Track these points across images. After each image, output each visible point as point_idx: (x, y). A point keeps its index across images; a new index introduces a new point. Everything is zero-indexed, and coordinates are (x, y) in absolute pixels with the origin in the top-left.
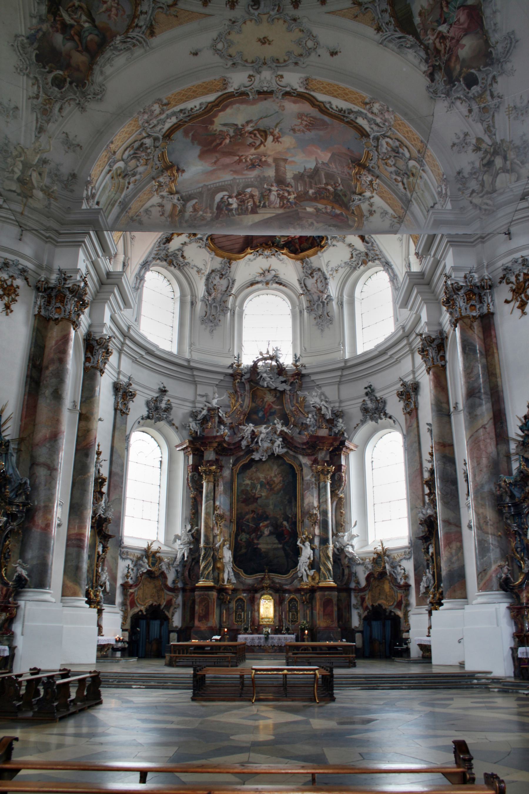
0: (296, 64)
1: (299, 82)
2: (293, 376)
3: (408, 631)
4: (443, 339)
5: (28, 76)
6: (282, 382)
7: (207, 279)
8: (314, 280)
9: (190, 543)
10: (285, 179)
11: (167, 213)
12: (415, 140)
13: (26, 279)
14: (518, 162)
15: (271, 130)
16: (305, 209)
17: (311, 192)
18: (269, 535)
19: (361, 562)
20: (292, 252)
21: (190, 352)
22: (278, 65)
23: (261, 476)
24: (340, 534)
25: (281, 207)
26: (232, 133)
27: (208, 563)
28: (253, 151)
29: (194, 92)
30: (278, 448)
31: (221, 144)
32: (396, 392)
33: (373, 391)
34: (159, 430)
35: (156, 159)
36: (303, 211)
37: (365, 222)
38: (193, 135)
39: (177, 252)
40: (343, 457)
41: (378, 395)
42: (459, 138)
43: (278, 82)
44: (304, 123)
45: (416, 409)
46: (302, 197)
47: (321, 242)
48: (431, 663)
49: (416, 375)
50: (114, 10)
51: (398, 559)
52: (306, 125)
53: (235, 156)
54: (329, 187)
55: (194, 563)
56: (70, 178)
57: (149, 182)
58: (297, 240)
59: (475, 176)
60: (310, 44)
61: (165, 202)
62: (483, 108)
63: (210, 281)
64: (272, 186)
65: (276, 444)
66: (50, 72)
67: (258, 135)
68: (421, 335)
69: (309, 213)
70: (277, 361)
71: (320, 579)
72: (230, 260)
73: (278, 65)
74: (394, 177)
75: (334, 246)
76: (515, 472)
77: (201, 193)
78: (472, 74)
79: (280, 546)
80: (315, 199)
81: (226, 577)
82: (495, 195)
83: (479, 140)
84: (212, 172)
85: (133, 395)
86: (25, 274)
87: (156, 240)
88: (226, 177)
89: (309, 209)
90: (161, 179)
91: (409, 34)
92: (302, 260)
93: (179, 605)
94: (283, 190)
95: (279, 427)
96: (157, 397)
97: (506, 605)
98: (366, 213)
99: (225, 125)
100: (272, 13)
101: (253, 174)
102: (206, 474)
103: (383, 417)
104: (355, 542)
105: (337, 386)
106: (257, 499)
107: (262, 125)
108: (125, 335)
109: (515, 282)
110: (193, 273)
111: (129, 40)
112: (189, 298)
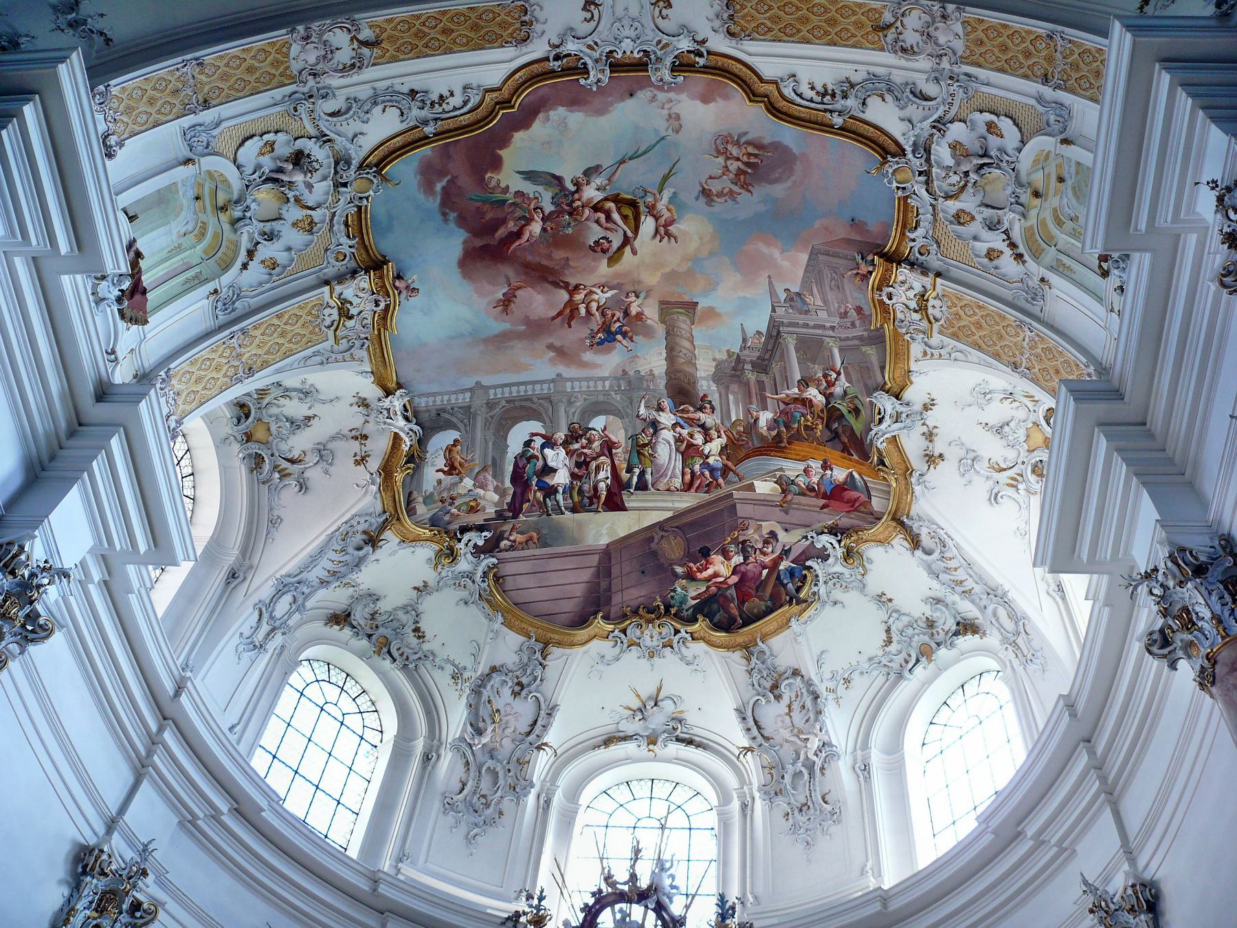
1: (711, 13)
7: (477, 691)
8: (782, 707)
10: (693, 382)
11: (374, 464)
15: (650, 199)
16: (751, 488)
17: (765, 417)
20: (718, 627)
25: (687, 487)
26: (549, 208)
28: (603, 269)
29: (445, 31)
31: (518, 234)
35: (339, 227)
36: (748, 494)
37: (917, 489)
38: (444, 188)
43: (660, 21)
44: (734, 166)
47: (798, 590)
52: (740, 172)
53: (556, 284)
54: (813, 393)
58: (733, 592)
61: (370, 429)
63: (486, 693)
64: (660, 409)
67: (616, 216)
69: (764, 502)
70: (660, 909)
75: (835, 603)
77: (467, 409)
80: (775, 446)
84: (500, 341)
87: (334, 528)
89: (764, 487)
90: (348, 290)
92: (747, 648)
94: (691, 422)
98: (917, 463)
99: (530, 176)
101: (609, 363)
108: (164, 717)
110: (440, 680)
112: (419, 745)
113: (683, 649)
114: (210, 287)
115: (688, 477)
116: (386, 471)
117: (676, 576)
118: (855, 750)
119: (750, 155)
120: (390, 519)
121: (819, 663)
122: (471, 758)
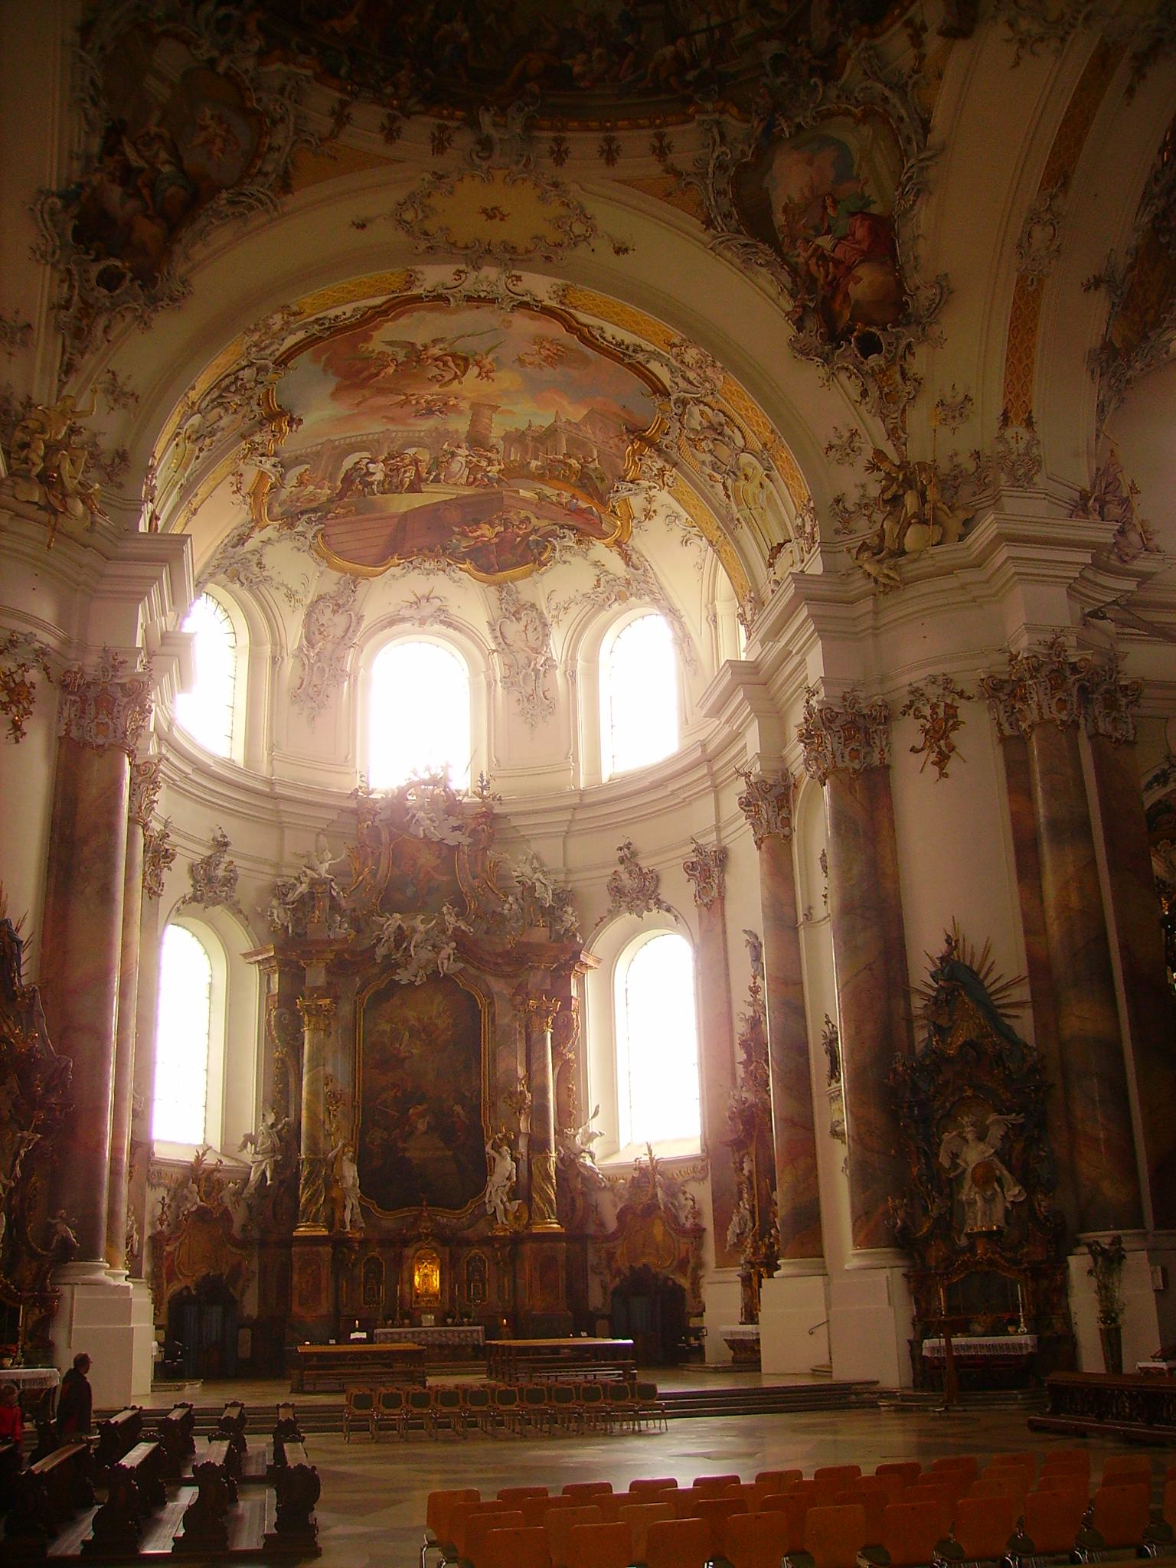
0: (548, 258)
2: (475, 817)
3: (701, 1315)
4: (787, 787)
5: (54, 266)
6: (454, 829)
7: (309, 615)
8: (521, 626)
9: (274, 1150)
12: (758, 425)
13: (46, 669)
14: (945, 507)
15: (478, 357)
16: (518, 492)
17: (534, 464)
18: (426, 1133)
19: (608, 1184)
21: (271, 762)
22: (514, 257)
23: (411, 1014)
24: (570, 1131)
26: (401, 358)
27: (316, 1191)
28: (436, 388)
30: (448, 964)
31: (377, 375)
32: (681, 861)
33: (634, 854)
34: (211, 923)
39: (249, 556)
40: (573, 981)
41: (645, 864)
42: (841, 437)
43: (511, 286)
44: (545, 352)
45: (722, 898)
46: (515, 473)
47: (541, 554)
48: (760, 1370)
49: (723, 834)
50: (218, 141)
51: (680, 1180)
52: (548, 356)
54: (573, 461)
55: (282, 1189)
56: (117, 461)
57: (235, 443)
59: (866, 512)
60: (578, 229)
62: (887, 394)
64: (459, 447)
65: (443, 954)
66: (96, 260)
68: (747, 775)
69: (523, 500)
71: (530, 1217)
72: (356, 578)
73: (514, 257)
74: (709, 471)
75: (565, 562)
76: (919, 1047)
77: (318, 454)
78: (873, 334)
79: (449, 1153)
80: (541, 478)
81: (348, 1216)
82: (902, 560)
83: (879, 454)
85: (169, 856)
86: (46, 659)
88: (374, 427)
90: (257, 438)
91: (763, 241)
92: (500, 586)
93: (253, 1272)
95: (450, 919)
96: (210, 857)
97: (902, 1270)
98: (637, 513)
99: (391, 343)
100: (514, 168)
102: (310, 1015)
103: (652, 906)
104: (594, 1146)
105: (561, 840)
106: (403, 1060)
107: (460, 348)
109: (929, 718)
111: (242, 198)
112: (267, 649)
113: (452, 573)
114: (179, 486)
115: (471, 480)
116: (254, 494)
117: (454, 533)
118: (566, 660)
119: (558, 350)
120: (256, 523)
121: (549, 599)
122: (306, 662)
